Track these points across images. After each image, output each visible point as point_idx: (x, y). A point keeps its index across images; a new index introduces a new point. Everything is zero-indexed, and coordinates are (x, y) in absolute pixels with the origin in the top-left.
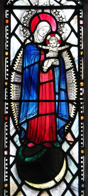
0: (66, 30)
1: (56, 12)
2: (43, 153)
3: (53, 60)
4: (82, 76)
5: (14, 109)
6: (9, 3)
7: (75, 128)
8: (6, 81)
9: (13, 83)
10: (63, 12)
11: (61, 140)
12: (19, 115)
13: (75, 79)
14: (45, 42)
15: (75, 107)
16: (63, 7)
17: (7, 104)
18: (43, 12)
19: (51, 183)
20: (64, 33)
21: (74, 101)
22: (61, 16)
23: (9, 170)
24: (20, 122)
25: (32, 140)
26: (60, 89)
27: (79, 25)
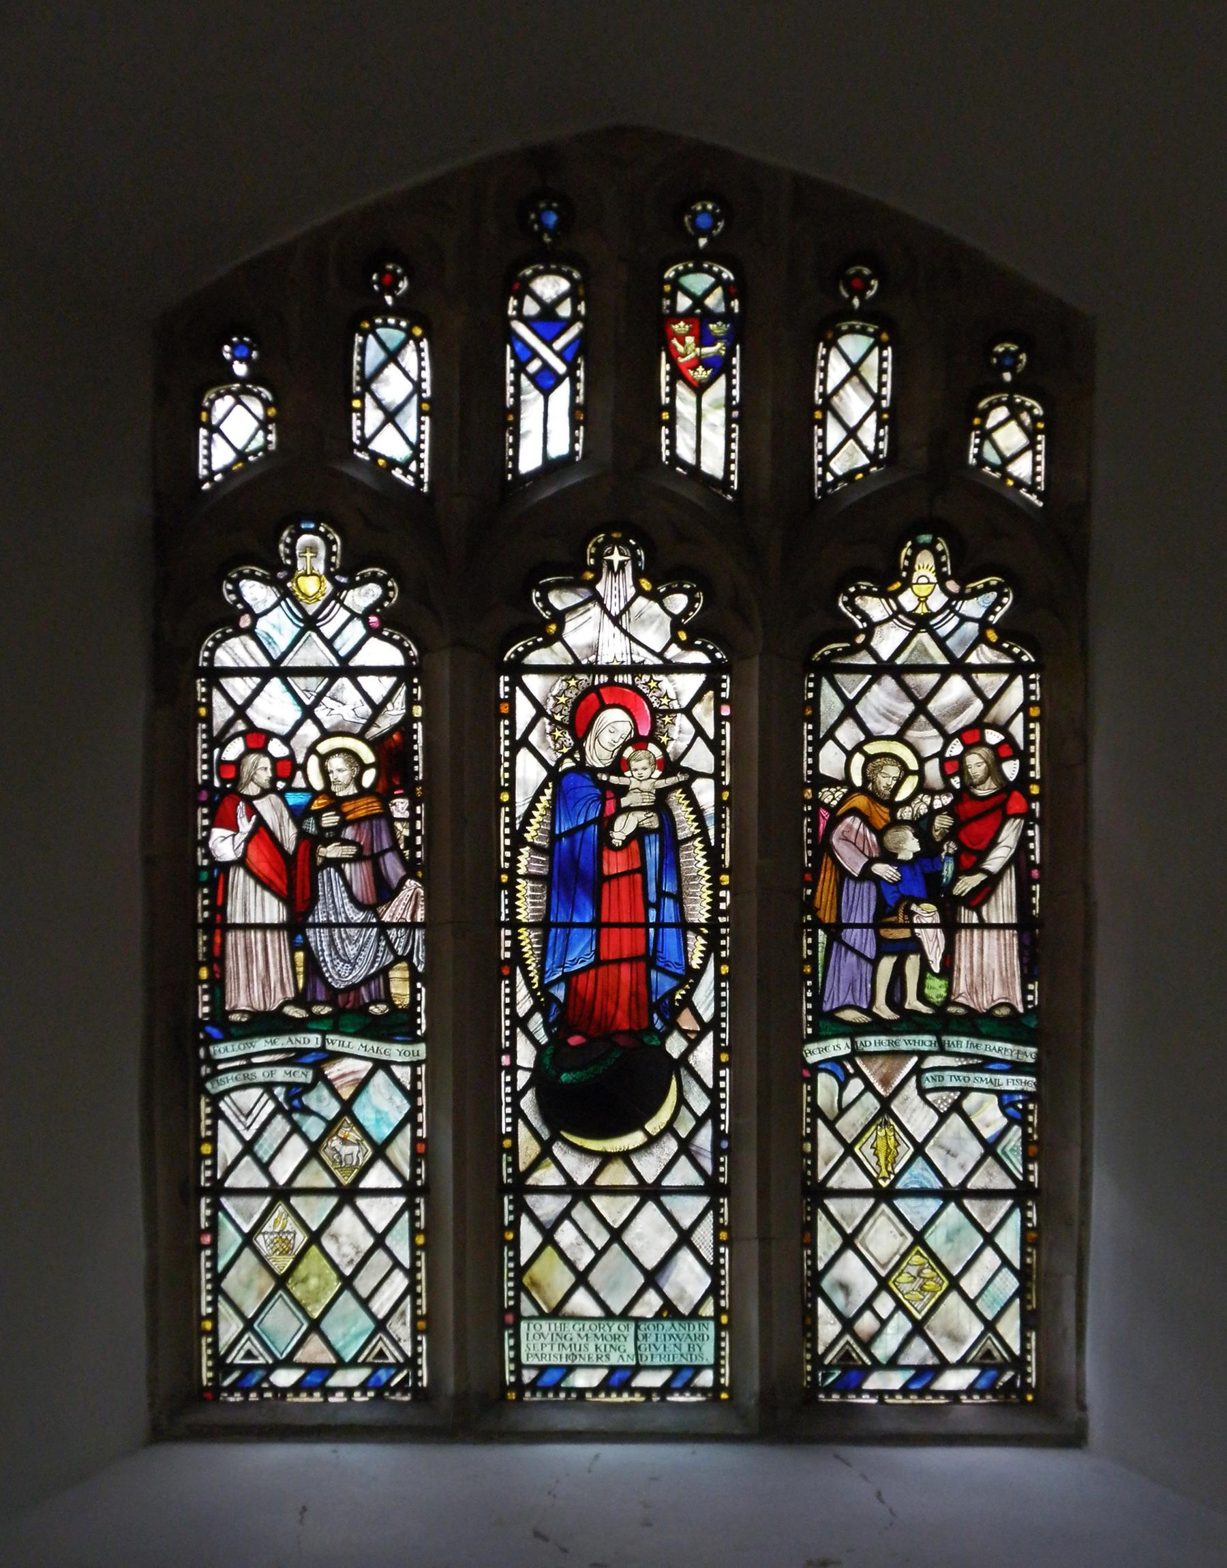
3: (641, 815)
4: (727, 857)
8: (505, 871)
9: (524, 877)
10: (671, 681)
14: (619, 765)
15: (704, 942)
17: (508, 933)
18: (611, 683)
19: (637, 1138)
22: (666, 694)
23: (515, 1104)
26: (661, 894)
27: (719, 719)
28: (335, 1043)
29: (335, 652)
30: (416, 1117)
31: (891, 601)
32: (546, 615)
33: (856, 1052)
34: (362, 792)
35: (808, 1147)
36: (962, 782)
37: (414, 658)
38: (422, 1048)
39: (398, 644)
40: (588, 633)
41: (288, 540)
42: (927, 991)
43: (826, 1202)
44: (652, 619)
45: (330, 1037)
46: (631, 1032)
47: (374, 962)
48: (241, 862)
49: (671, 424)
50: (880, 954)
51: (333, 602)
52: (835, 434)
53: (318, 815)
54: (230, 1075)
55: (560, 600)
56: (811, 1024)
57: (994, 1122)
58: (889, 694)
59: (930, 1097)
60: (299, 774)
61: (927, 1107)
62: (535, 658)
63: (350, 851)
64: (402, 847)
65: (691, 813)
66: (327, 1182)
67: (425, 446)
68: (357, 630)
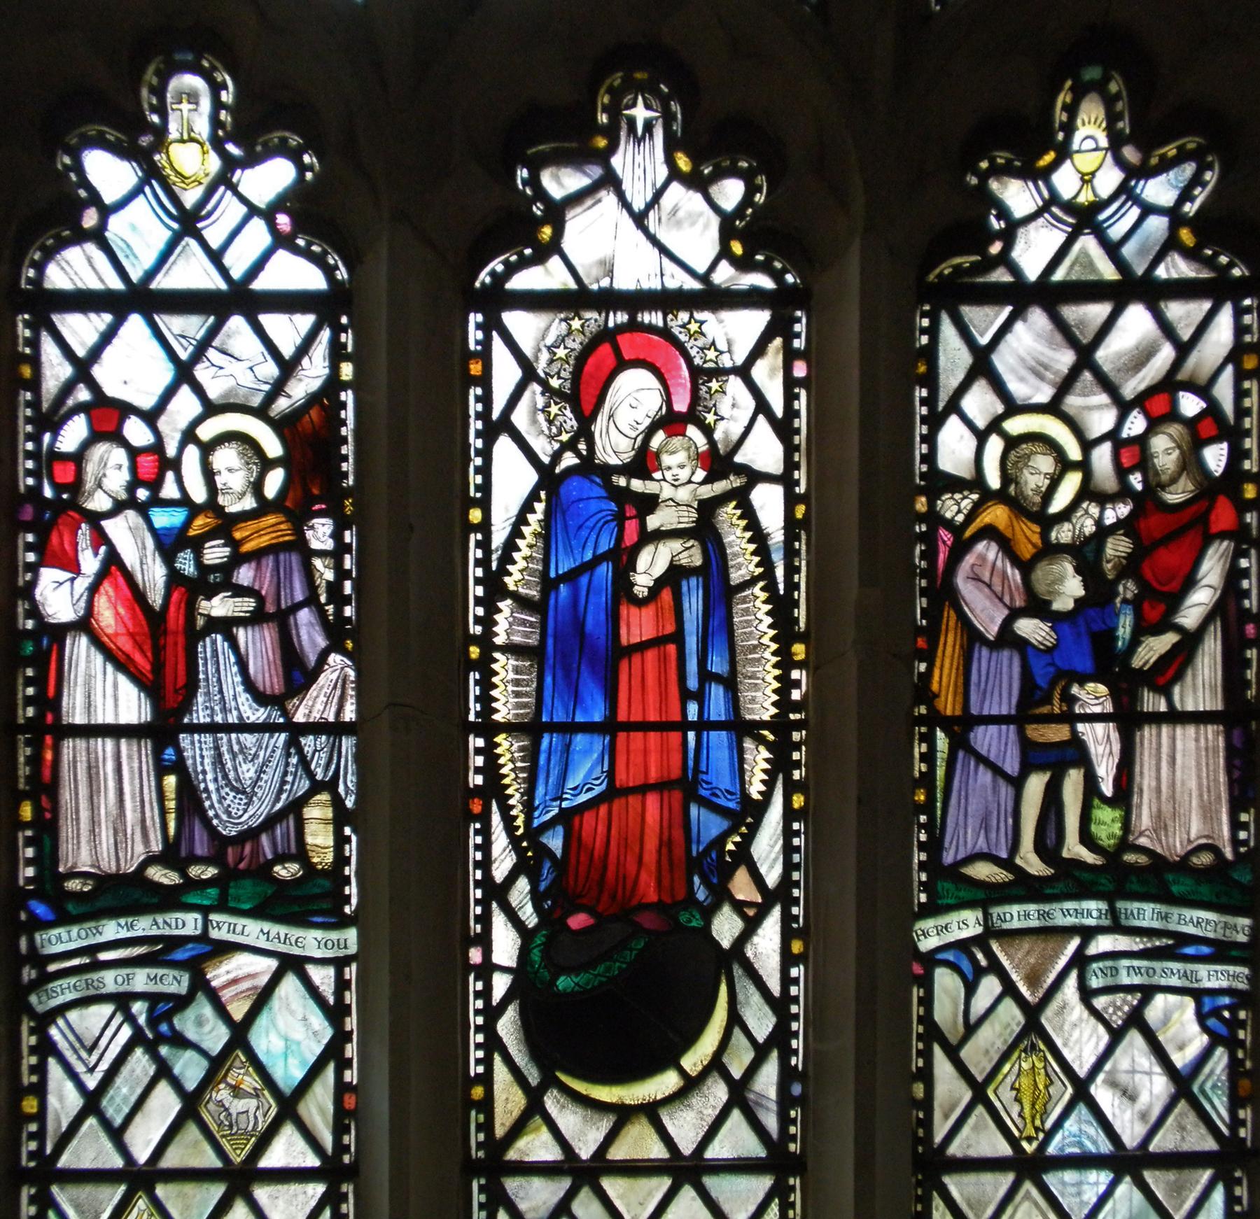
0: (733, 405)
1: (689, 322)
2: (630, 956)
3: (676, 545)
4: (801, 613)
5: (511, 766)
6: (483, 283)
7: (767, 847)
8: (475, 640)
10: (721, 322)
11: (709, 900)
12: (530, 793)
13: (770, 627)
14: (644, 462)
15: (767, 755)
16: (714, 298)
17: (480, 742)
18: (633, 326)
19: (668, 1082)
20: (722, 419)
21: (762, 724)
22: (713, 343)
24: (536, 823)
25: (585, 901)
26: (706, 676)
27: (790, 384)
28: (224, 927)
29: (224, 272)
30: (343, 1051)
31: (1040, 183)
33: (990, 932)
34: (264, 507)
35: (919, 1090)
36: (1145, 481)
38: (351, 935)
39: (319, 261)
40: (600, 242)
41: (155, 81)
42: (1093, 828)
43: (947, 1180)
44: (693, 218)
45: (214, 917)
46: (659, 906)
47: (281, 791)
48: (85, 624)
50: (1028, 767)
51: (222, 188)
53: (197, 545)
54: (64, 982)
55: (561, 182)
56: (925, 887)
57: (1190, 1041)
58: (1039, 336)
59: (1100, 1002)
60: (170, 476)
61: (1093, 1021)
63: (246, 605)
64: (323, 599)
65: (750, 541)
66: (210, 1160)
68: (257, 236)
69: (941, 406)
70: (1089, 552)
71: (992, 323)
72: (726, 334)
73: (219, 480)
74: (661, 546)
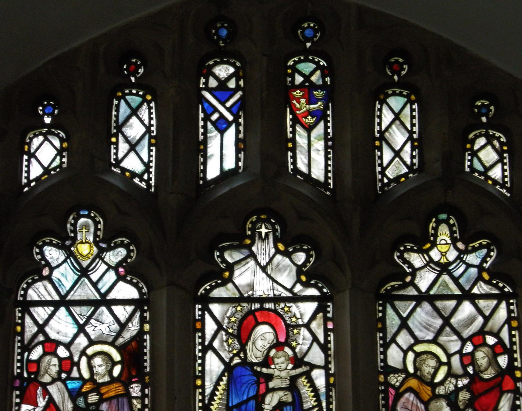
0: (304, 339)
1: (285, 307)
3: (281, 393)
6: (201, 293)
10: (297, 307)
14: (267, 361)
18: (262, 309)
20: (299, 344)
27: (326, 331)
29: (98, 290)
31: (425, 255)
32: (223, 266)
34: (113, 380)
36: (474, 370)
37: (145, 294)
39: (136, 285)
40: (249, 277)
41: (73, 222)
44: (285, 268)
49: (294, 150)
51: (98, 260)
52: (388, 155)
53: (86, 395)
58: (427, 313)
60: (75, 368)
62: (217, 293)
65: (312, 392)
67: (153, 164)
68: (111, 276)
69: (388, 340)
70: (452, 397)
71: (408, 308)
72: (300, 312)
73: (95, 370)
74: (275, 394)
